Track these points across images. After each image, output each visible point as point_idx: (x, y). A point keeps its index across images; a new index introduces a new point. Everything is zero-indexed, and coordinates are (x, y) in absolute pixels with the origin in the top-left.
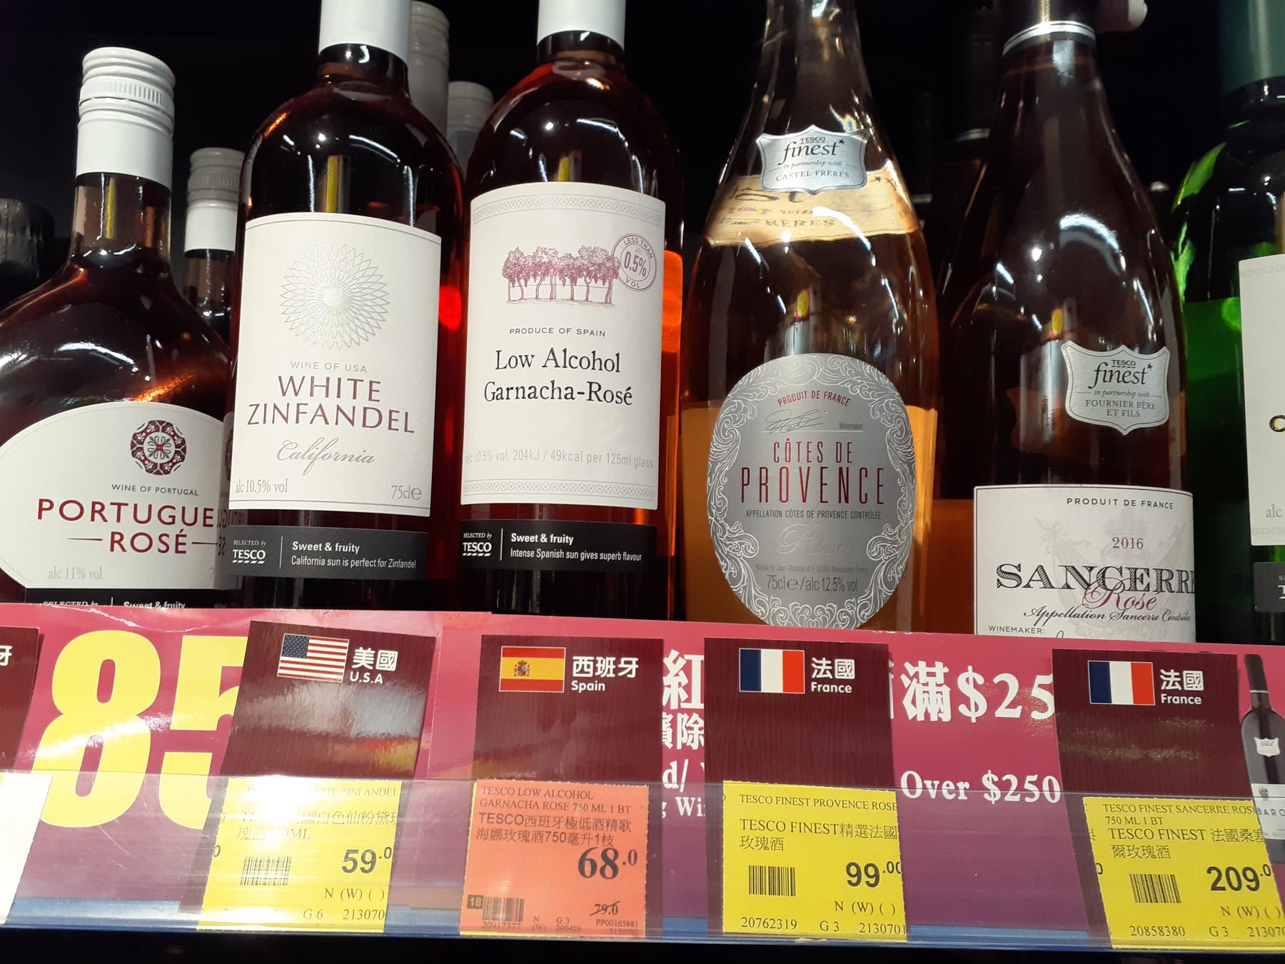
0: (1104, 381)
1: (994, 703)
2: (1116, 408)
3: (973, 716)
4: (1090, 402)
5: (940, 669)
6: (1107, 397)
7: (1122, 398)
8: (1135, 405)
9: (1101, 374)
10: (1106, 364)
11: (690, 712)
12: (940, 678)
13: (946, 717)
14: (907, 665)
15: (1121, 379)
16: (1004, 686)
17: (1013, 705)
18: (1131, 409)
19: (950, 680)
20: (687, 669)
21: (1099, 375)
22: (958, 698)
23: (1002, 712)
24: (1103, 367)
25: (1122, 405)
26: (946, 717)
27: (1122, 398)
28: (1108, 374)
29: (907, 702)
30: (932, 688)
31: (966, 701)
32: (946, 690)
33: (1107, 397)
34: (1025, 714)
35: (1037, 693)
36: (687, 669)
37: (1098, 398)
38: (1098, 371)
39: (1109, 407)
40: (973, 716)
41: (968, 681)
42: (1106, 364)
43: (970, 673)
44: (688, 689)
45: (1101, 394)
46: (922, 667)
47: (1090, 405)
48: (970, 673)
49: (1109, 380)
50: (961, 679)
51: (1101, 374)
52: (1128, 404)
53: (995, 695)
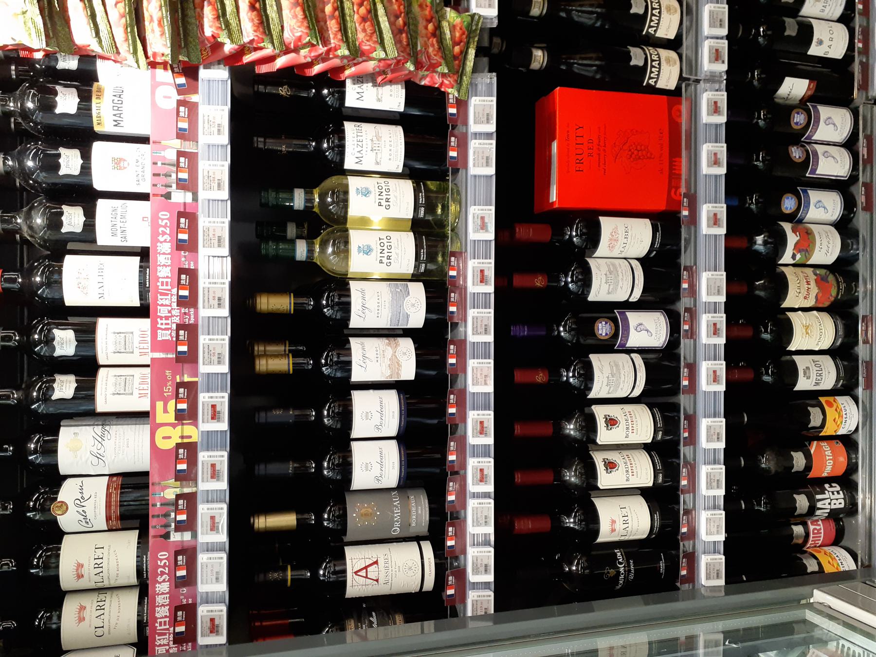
1: (166, 574)
3: (168, 578)
5: (157, 585)
11: (169, 638)
12: (160, 585)
13: (168, 583)
14: (158, 592)
16: (161, 571)
17: (165, 569)
19: (160, 583)
20: (159, 640)
22: (164, 581)
23: (167, 571)
26: (168, 583)
29: (165, 592)
30: (162, 587)
31: (164, 579)
32: (162, 584)
34: (167, 566)
35: (162, 564)
36: (159, 640)
40: (168, 578)
41: (160, 579)
43: (158, 579)
44: (164, 639)
46: (157, 589)
48: (158, 579)
50: (159, 581)
53: (162, 573)
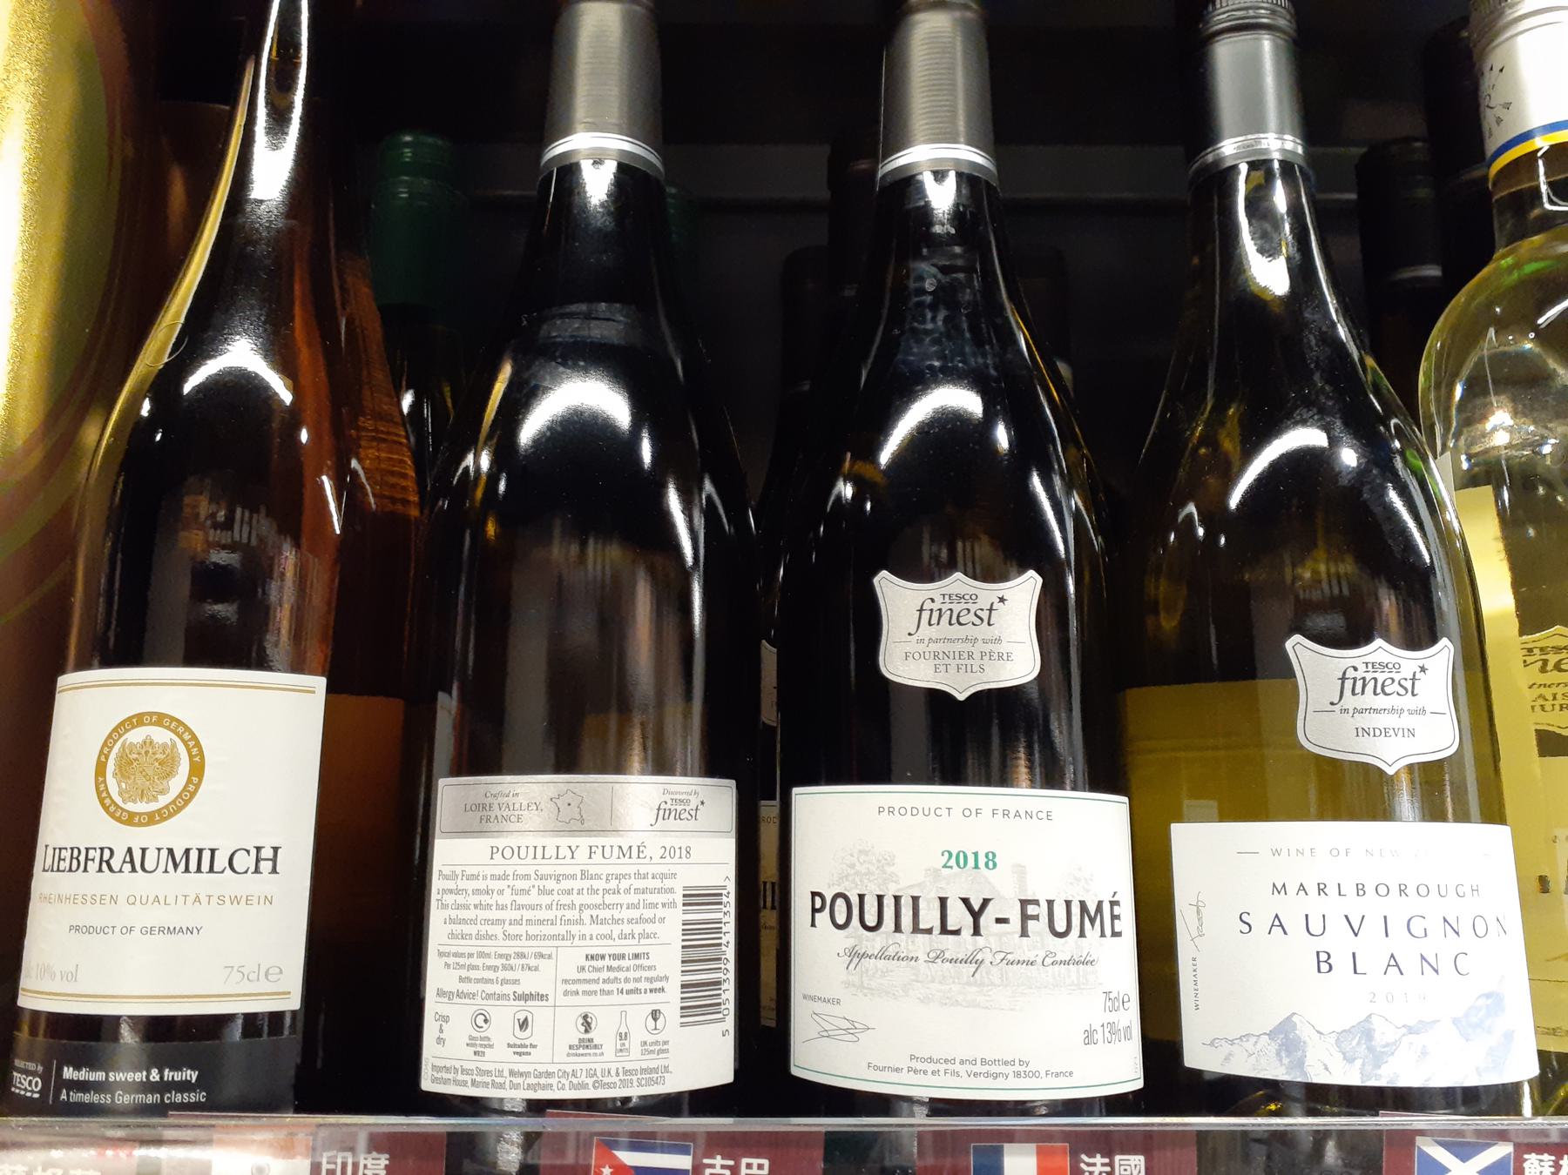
0: (930, 624)
2: (947, 661)
4: (911, 656)
6: (933, 647)
7: (959, 647)
8: (977, 656)
9: (926, 615)
10: (933, 600)
15: (954, 620)
18: (971, 661)
21: (923, 616)
24: (928, 605)
25: (957, 657)
27: (959, 647)
28: (936, 614)
33: (933, 647)
37: (921, 648)
38: (921, 610)
39: (937, 662)
42: (933, 600)
45: (926, 642)
47: (910, 659)
49: (936, 622)
51: (926, 615)
52: (966, 655)
